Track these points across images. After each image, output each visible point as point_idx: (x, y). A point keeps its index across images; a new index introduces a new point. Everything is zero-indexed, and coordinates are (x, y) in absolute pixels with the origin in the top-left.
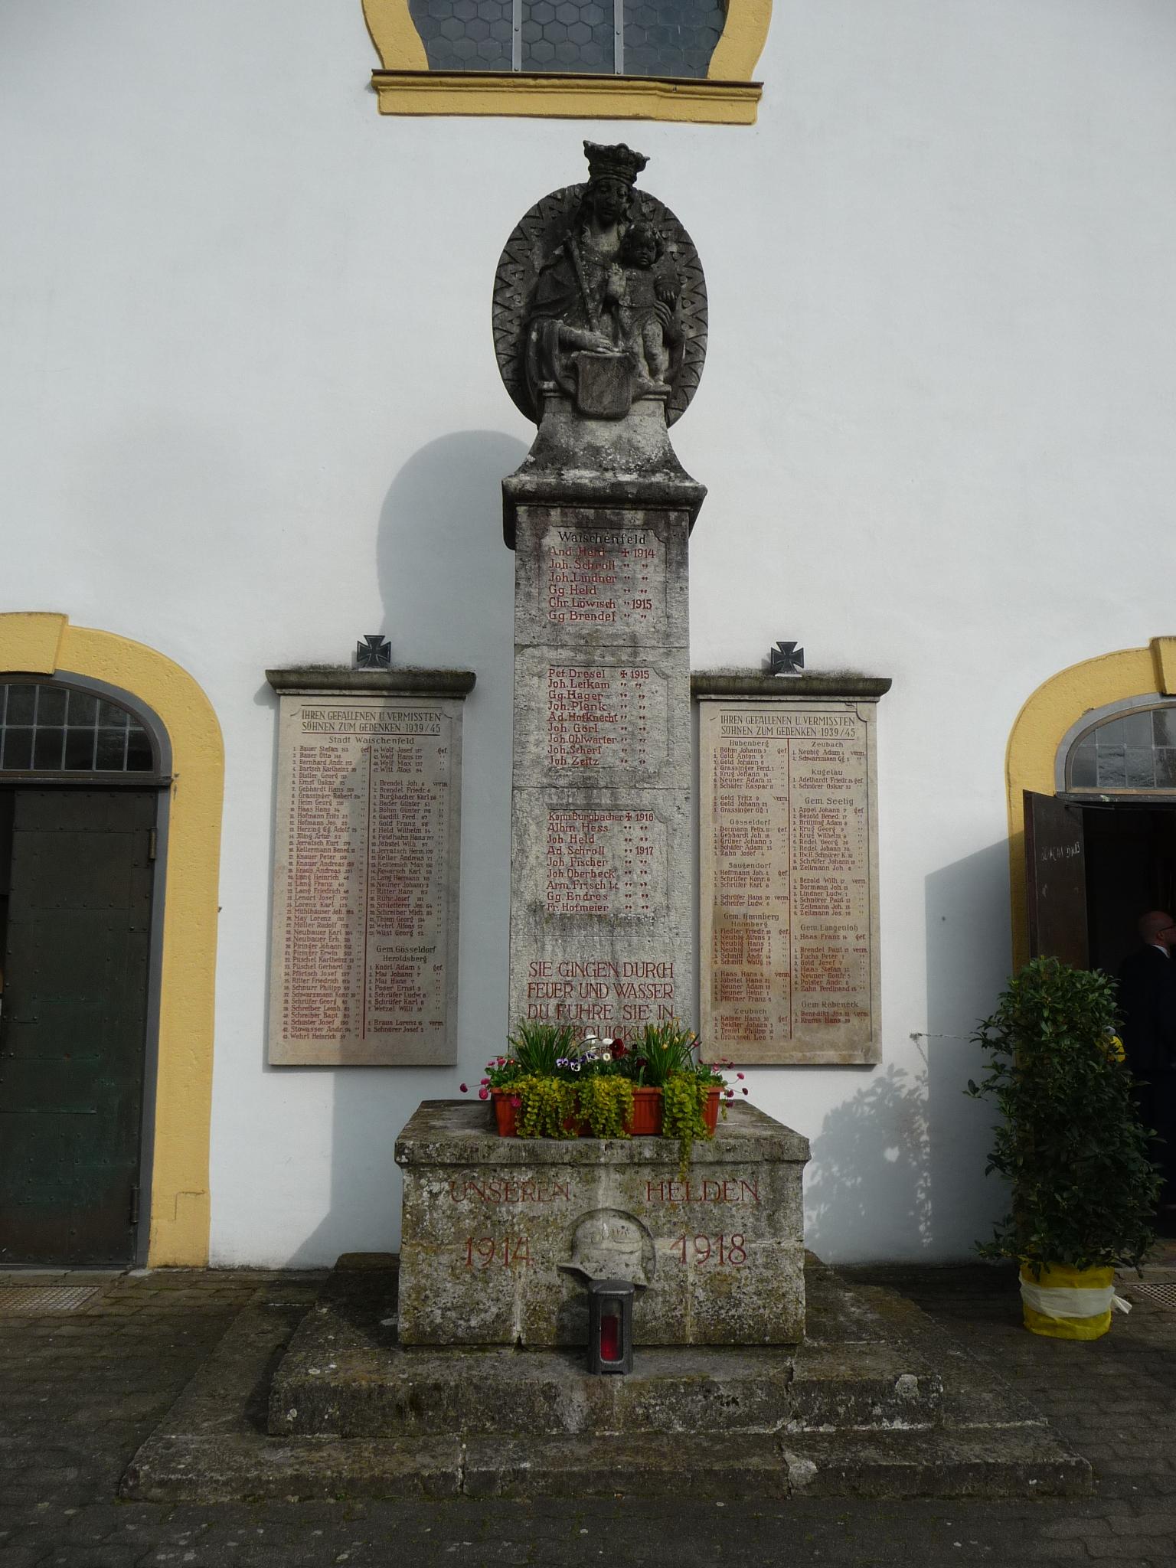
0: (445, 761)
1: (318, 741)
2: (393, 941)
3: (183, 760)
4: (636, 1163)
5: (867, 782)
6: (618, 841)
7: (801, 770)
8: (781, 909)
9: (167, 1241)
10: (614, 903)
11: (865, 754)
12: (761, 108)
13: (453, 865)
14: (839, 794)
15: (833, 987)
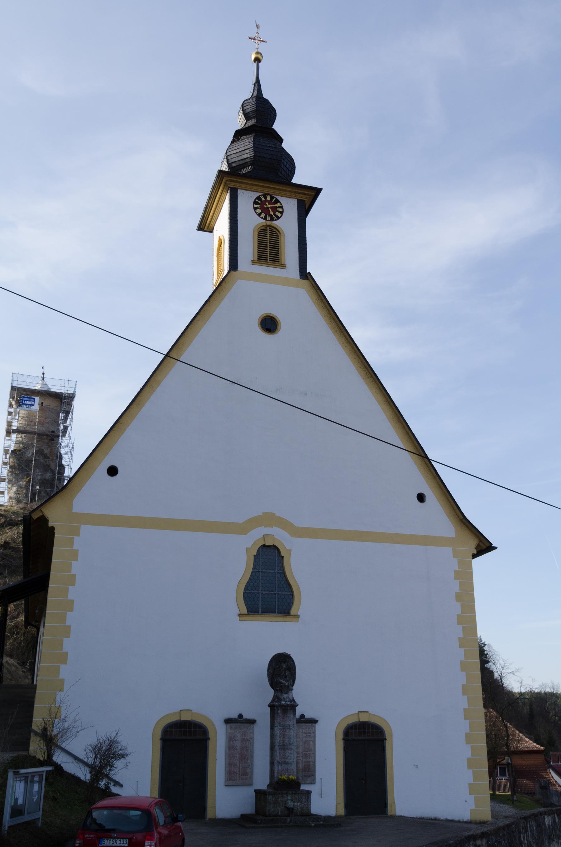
0: (251, 734)
1: (232, 732)
2: (244, 764)
3: (211, 735)
4: (292, 794)
5: (314, 737)
6: (288, 752)
7: (305, 735)
8: (301, 758)
9: (210, 814)
10: (287, 761)
11: (314, 732)
12: (299, 619)
13: (252, 752)
14: (310, 739)
15: (309, 771)
